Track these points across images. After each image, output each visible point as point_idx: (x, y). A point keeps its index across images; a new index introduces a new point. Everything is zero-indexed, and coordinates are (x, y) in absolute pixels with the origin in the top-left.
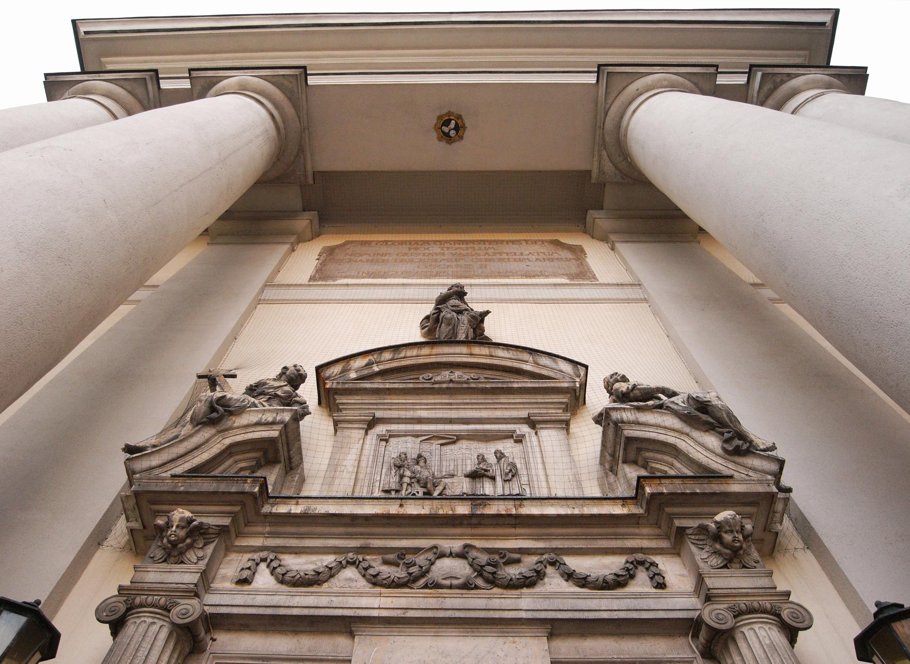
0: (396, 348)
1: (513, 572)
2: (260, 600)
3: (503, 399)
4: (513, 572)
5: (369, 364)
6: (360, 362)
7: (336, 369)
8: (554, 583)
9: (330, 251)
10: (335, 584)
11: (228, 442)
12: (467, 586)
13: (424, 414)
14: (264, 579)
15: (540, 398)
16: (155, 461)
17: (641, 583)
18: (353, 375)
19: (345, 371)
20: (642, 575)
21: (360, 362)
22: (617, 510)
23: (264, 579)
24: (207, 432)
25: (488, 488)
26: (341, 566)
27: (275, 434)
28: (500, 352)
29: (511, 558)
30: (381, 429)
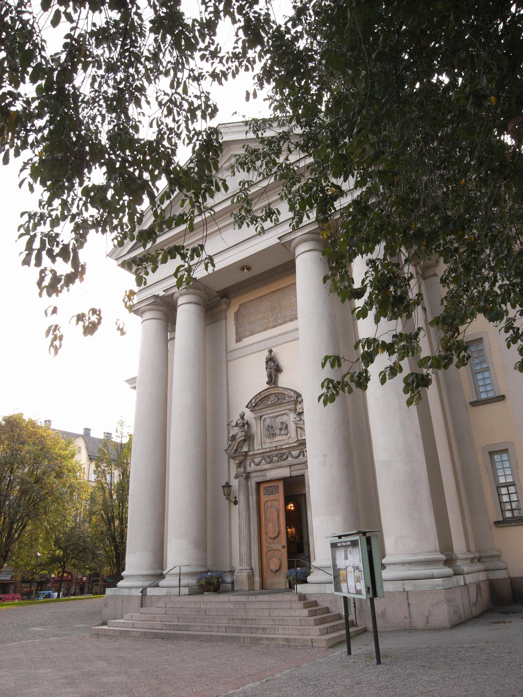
0: (259, 393)
1: (284, 457)
2: (253, 469)
3: (282, 405)
4: (284, 457)
5: (256, 400)
6: (254, 400)
7: (250, 405)
8: (290, 458)
9: (237, 315)
10: (262, 464)
11: (237, 442)
12: (278, 461)
13: (269, 412)
14: (253, 465)
15: (289, 403)
16: (229, 451)
17: (301, 457)
18: (254, 405)
19: (252, 404)
20: (301, 454)
21: (254, 400)
22: (296, 444)
23: (253, 465)
24: (234, 442)
25: (282, 432)
26: (261, 460)
27: (243, 438)
28: (280, 389)
29: (284, 454)
30: (263, 418)
